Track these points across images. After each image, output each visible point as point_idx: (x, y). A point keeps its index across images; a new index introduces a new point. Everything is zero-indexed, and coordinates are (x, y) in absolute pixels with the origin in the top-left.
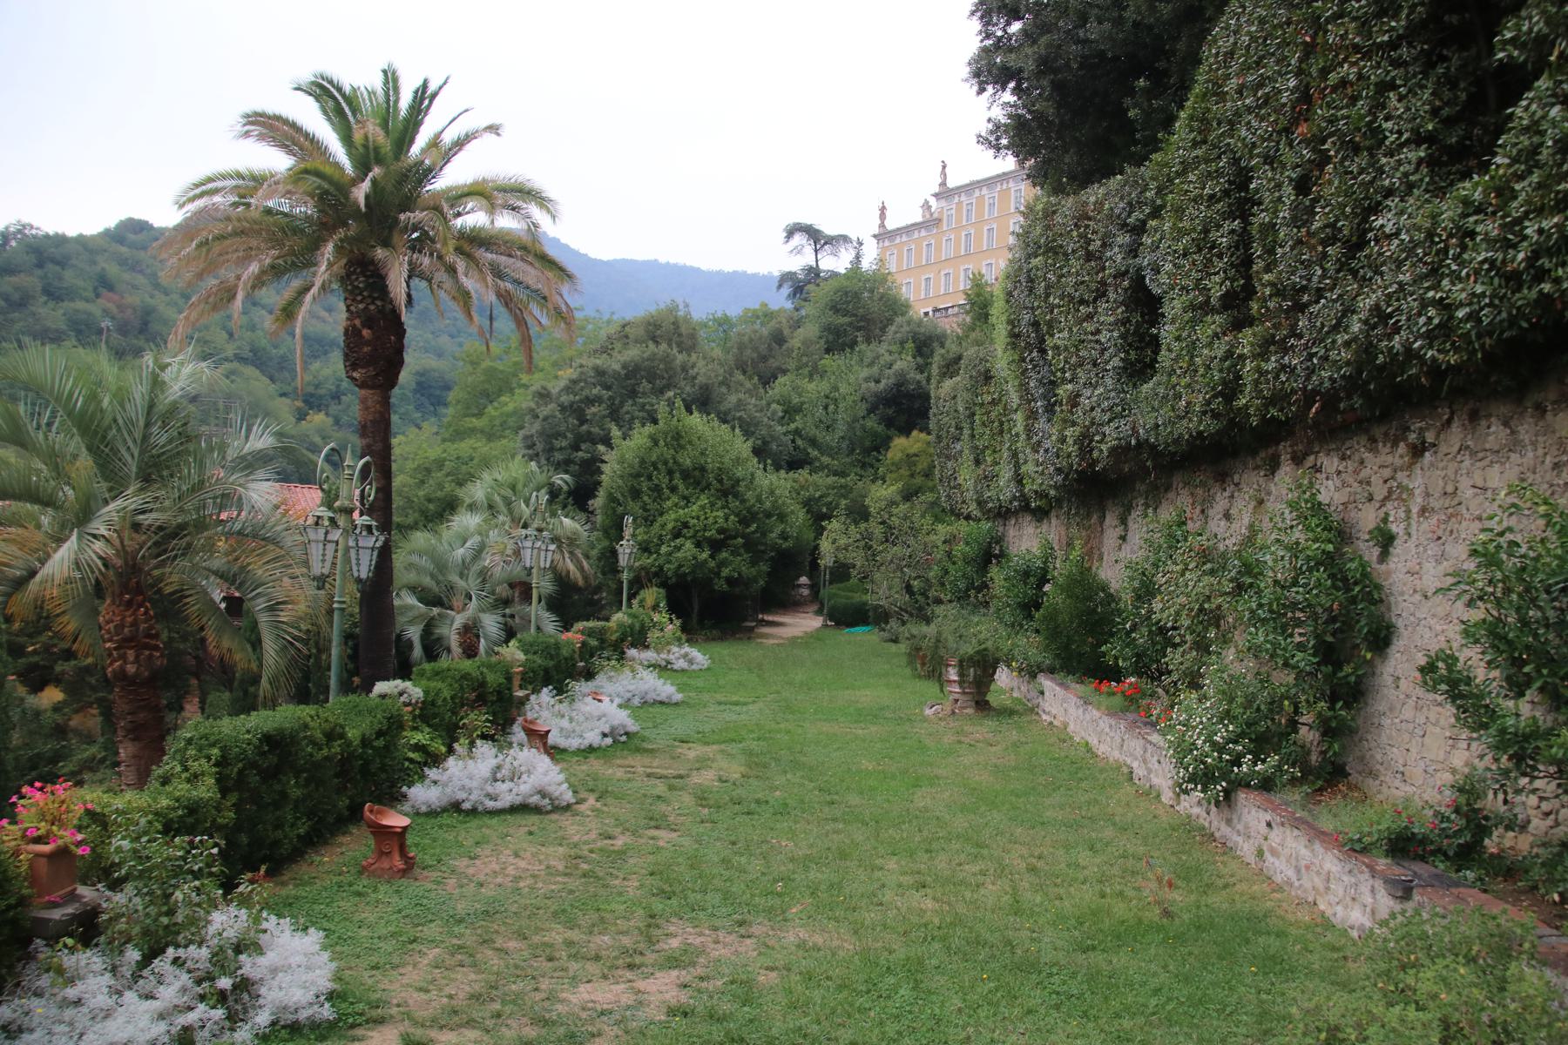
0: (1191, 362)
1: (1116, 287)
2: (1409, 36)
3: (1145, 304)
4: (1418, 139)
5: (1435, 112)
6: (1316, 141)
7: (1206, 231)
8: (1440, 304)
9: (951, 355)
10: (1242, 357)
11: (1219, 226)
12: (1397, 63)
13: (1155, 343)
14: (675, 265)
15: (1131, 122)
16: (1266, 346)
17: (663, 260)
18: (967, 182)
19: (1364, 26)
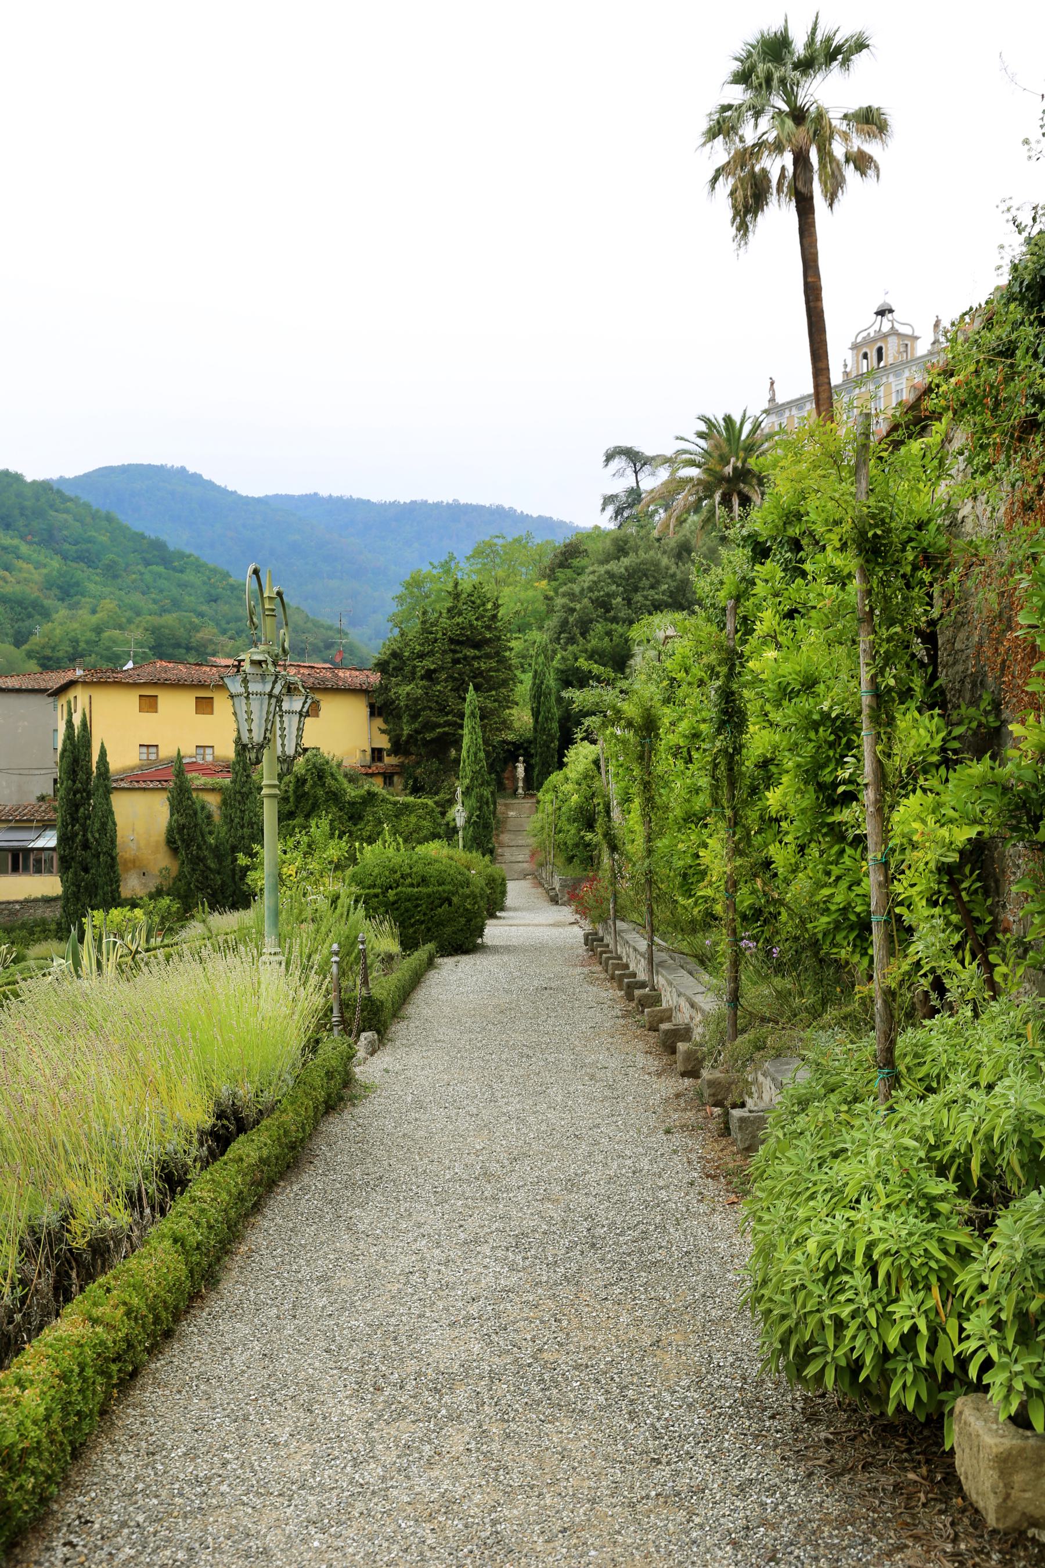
14: (340, 499)
17: (324, 493)
18: (798, 396)
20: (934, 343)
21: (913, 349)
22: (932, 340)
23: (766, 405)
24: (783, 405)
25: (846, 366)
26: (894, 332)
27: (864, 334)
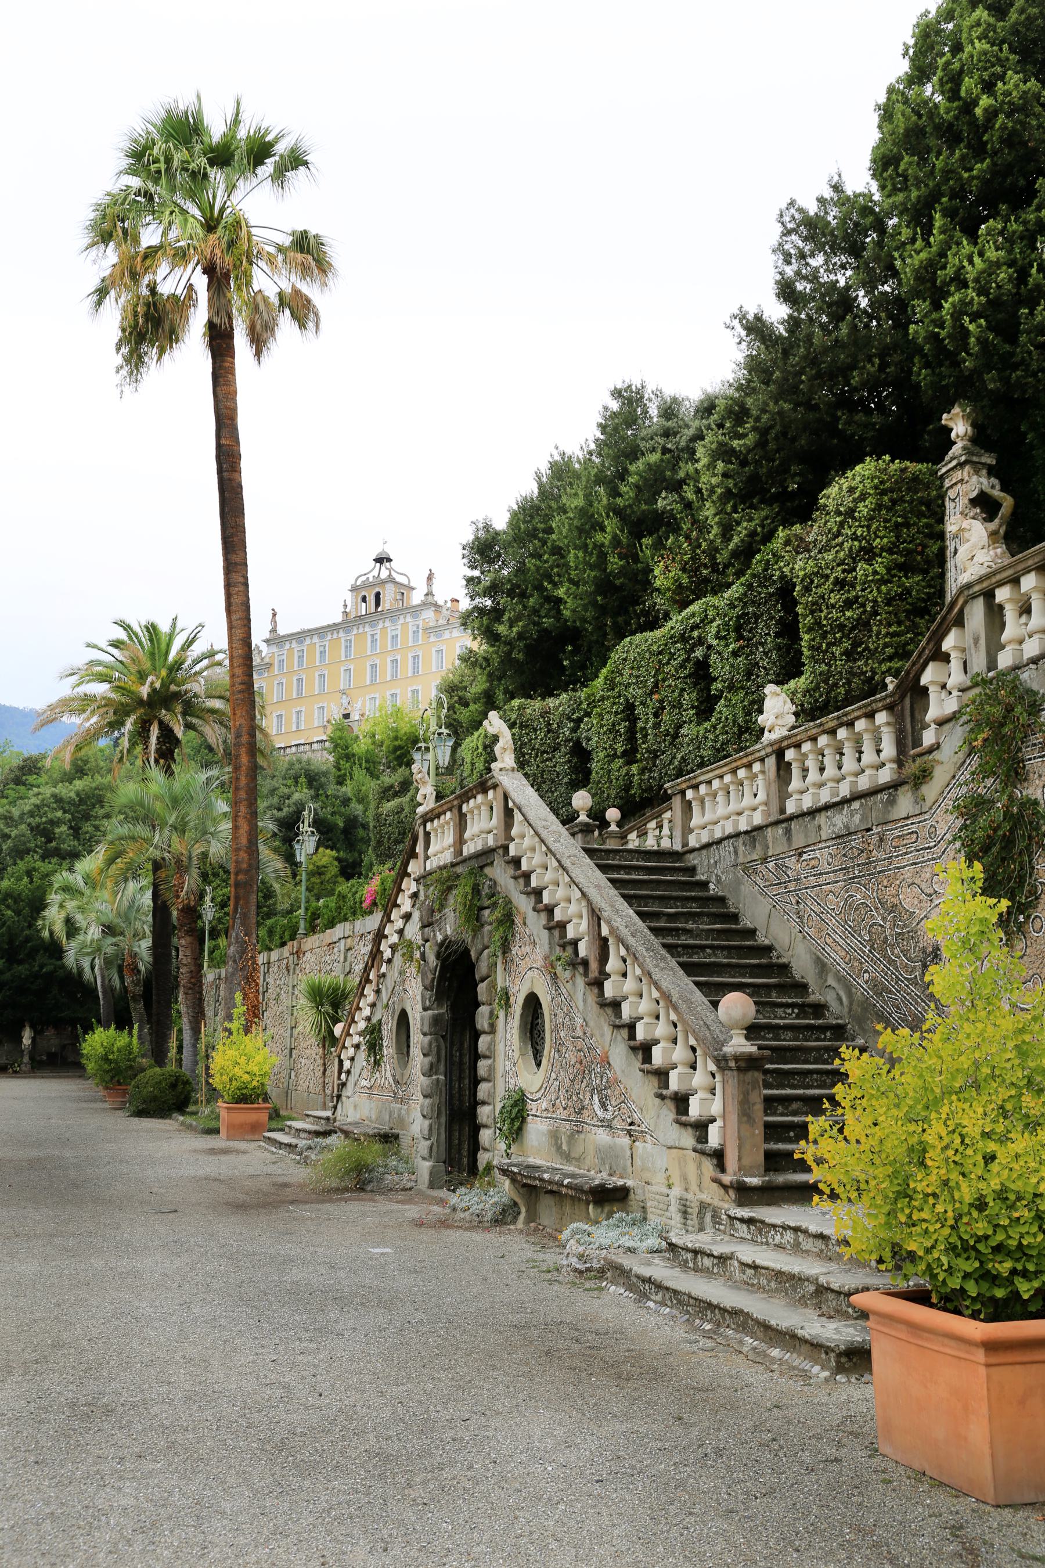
0: (609, 777)
1: (566, 746)
2: (690, 676)
3: (581, 755)
4: (693, 707)
5: (697, 700)
6: (661, 702)
7: (614, 725)
8: (700, 756)
9: (386, 785)
10: (634, 775)
11: (619, 724)
12: (686, 683)
13: (589, 772)
15: (564, 667)
16: (642, 771)
19: (677, 671)
20: (427, 595)
21: (409, 598)
22: (425, 592)
23: (267, 636)
24: (284, 636)
25: (346, 606)
26: (391, 580)
27: (364, 578)
